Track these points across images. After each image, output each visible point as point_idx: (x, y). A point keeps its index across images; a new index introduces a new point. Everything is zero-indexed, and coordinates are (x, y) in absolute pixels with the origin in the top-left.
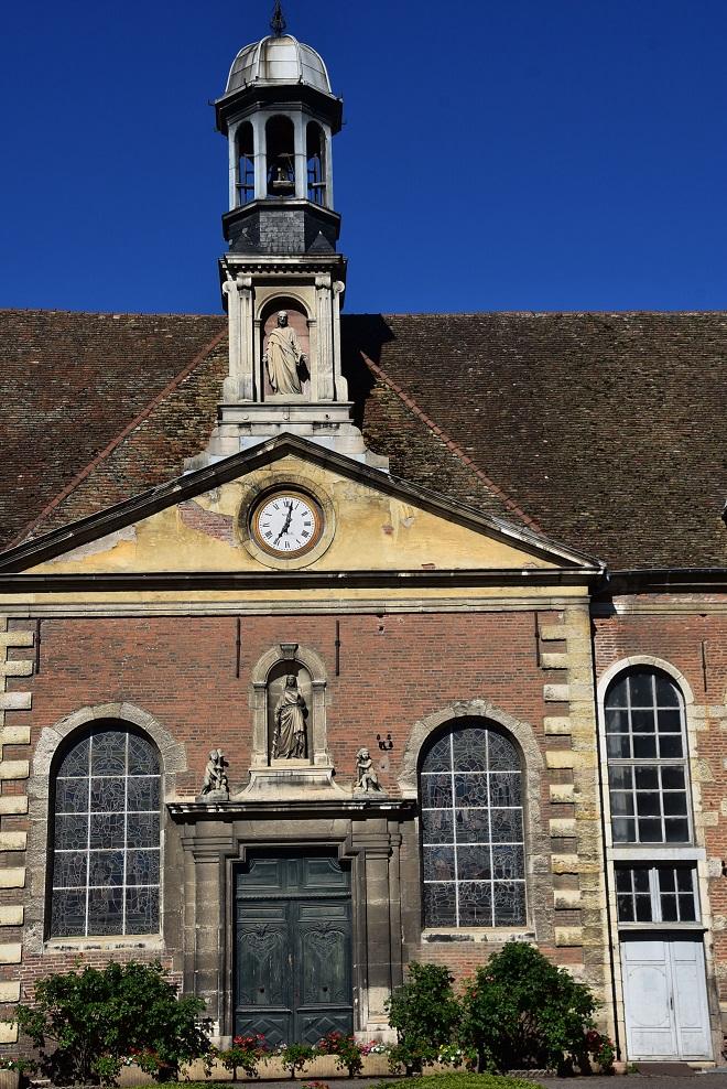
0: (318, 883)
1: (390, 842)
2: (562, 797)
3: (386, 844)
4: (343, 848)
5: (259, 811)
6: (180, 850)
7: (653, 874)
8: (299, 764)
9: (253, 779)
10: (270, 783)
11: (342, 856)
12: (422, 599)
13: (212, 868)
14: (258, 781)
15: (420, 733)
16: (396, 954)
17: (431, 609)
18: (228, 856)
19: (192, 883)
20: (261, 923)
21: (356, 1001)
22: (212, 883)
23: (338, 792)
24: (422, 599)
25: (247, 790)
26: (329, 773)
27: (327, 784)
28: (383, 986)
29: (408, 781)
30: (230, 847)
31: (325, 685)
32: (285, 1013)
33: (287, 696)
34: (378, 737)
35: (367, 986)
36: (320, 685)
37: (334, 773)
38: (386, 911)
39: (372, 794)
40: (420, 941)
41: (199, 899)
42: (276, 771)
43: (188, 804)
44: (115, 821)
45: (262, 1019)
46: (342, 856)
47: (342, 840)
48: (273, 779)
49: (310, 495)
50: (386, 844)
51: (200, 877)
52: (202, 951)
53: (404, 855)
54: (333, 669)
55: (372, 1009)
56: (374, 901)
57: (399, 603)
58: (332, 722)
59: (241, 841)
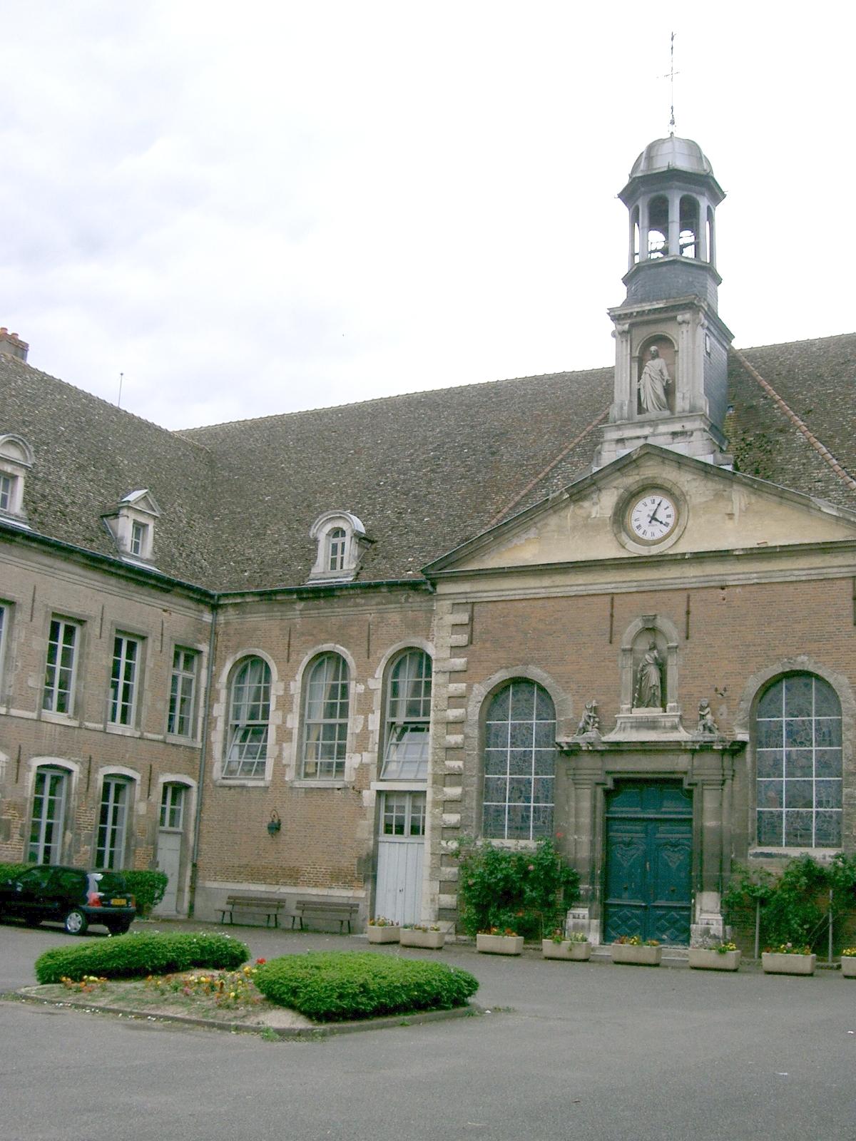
0: (671, 808)
1: (723, 775)
2: (524, 688)
3: (721, 777)
4: (686, 782)
5: (617, 749)
6: (565, 778)
7: (689, 836)
8: (656, 712)
9: (618, 725)
10: (632, 727)
11: (686, 787)
12: (756, 573)
13: (586, 793)
14: (623, 726)
15: (754, 684)
16: (727, 866)
17: (763, 581)
18: (597, 784)
19: (573, 804)
20: (626, 837)
21: (693, 901)
22: (586, 804)
23: (682, 735)
24: (756, 573)
25: (614, 732)
26: (677, 720)
27: (674, 728)
28: (714, 891)
29: (743, 726)
30: (599, 777)
31: (677, 647)
32: (641, 906)
33: (647, 656)
34: (716, 690)
35: (701, 890)
36: (672, 648)
37: (681, 717)
38: (719, 832)
39: (708, 737)
40: (746, 856)
41: (577, 816)
42: (636, 718)
43: (567, 743)
44: (332, 746)
45: (626, 912)
46: (686, 787)
47: (685, 773)
48: (634, 724)
49: (657, 488)
50: (721, 777)
51: (578, 801)
52: (579, 855)
53: (737, 787)
54: (683, 635)
55: (705, 908)
56: (710, 823)
57: (737, 577)
58: (682, 677)
59: (608, 773)
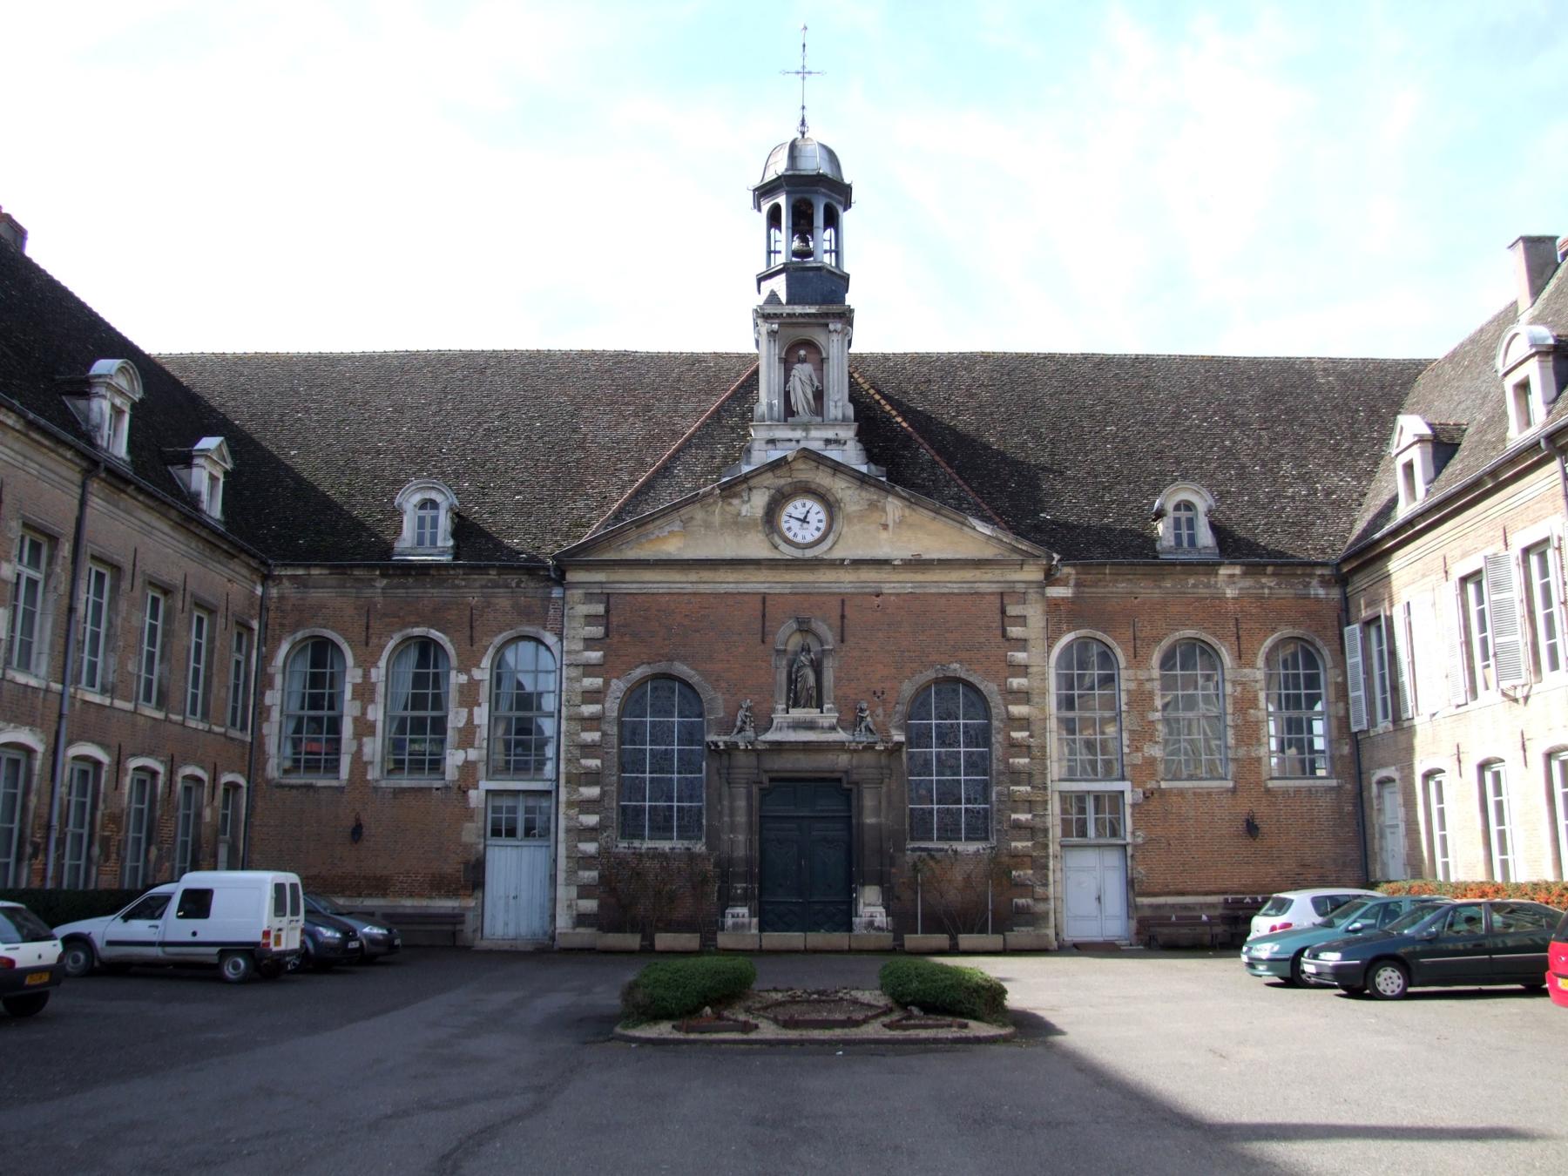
8: (811, 713)
13: (741, 791)
23: (841, 735)
27: (832, 728)
29: (899, 727)
35: (863, 885)
38: (878, 827)
51: (732, 798)
56: (870, 820)
58: (838, 679)
